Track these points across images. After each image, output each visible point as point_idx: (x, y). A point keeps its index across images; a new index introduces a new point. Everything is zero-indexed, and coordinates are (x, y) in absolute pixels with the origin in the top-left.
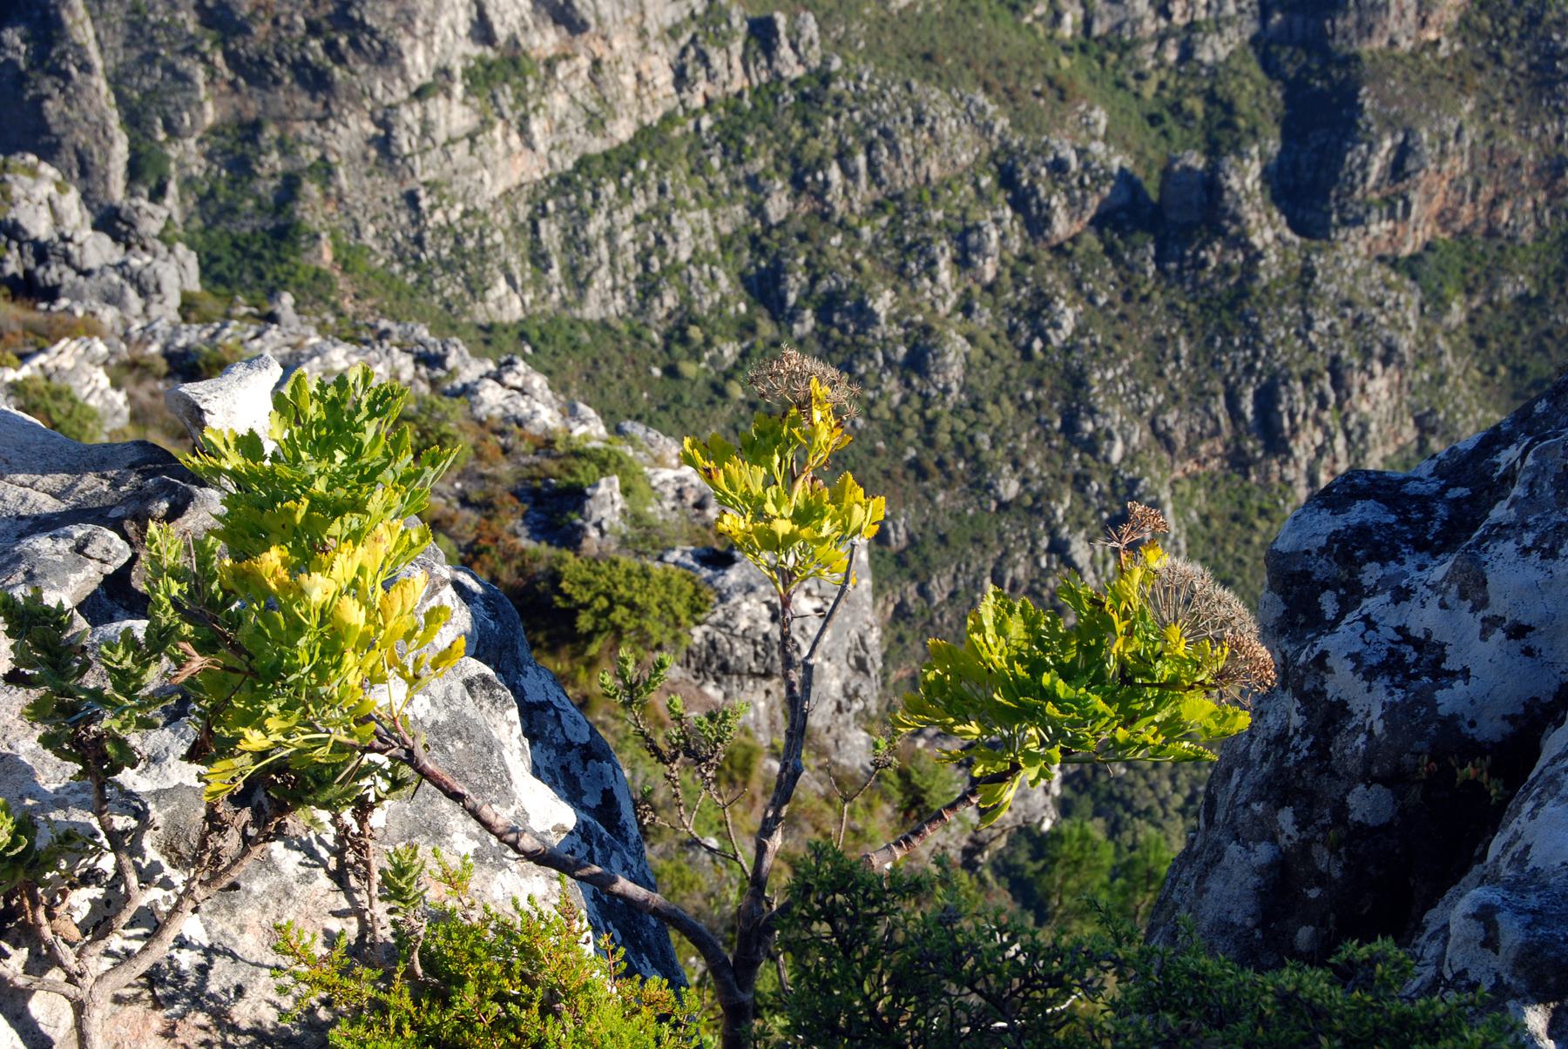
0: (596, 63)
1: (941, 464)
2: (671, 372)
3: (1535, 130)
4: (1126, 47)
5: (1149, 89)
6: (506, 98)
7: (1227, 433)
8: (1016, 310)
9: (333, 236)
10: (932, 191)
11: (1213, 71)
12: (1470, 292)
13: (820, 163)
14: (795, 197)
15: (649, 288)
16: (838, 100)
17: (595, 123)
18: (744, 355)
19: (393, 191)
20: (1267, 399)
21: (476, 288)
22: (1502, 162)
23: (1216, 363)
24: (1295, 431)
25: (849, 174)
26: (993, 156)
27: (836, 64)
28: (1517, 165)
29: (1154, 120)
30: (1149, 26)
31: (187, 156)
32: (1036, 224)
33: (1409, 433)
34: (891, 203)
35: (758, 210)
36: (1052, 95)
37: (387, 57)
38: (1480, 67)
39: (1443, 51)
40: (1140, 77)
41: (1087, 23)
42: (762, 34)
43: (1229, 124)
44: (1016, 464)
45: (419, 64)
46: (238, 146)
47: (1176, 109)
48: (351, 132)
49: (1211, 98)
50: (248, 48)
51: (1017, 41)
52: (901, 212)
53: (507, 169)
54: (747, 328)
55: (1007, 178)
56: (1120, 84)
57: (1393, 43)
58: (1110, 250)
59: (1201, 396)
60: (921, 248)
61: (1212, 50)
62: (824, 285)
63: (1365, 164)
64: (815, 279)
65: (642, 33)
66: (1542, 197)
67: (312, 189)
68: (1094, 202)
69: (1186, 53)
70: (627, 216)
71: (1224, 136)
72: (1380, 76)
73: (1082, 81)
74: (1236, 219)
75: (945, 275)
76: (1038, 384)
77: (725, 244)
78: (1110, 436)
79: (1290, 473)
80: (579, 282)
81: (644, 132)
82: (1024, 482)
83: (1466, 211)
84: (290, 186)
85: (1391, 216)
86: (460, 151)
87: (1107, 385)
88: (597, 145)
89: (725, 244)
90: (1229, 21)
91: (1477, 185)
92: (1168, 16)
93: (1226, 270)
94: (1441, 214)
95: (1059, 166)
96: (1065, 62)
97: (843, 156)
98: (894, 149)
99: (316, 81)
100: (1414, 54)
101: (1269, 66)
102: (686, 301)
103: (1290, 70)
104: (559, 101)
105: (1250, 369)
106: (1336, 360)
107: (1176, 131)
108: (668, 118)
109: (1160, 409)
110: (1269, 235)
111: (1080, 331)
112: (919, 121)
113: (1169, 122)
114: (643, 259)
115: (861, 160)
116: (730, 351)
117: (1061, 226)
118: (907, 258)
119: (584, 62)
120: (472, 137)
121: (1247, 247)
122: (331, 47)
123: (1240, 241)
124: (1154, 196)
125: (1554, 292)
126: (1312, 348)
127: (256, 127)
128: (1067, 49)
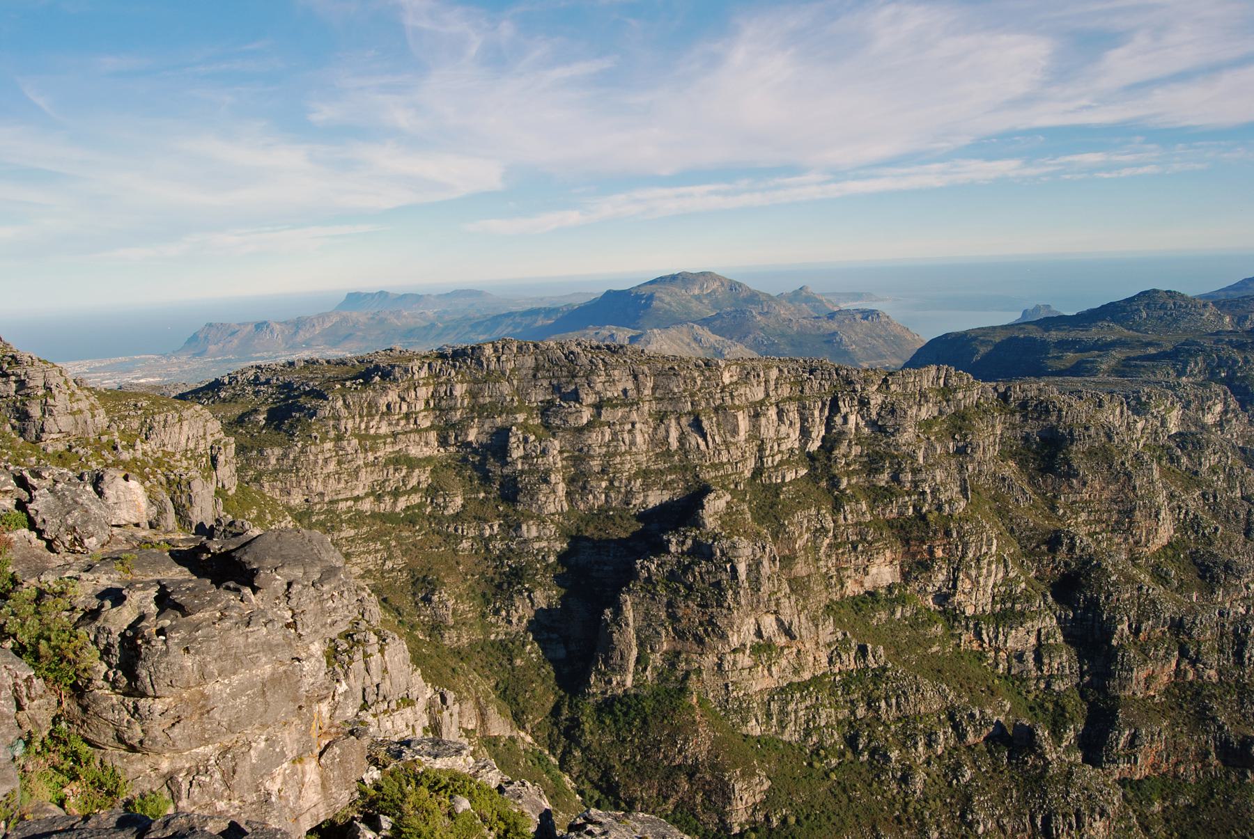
0: (799, 651)
1: (908, 820)
2: (810, 764)
3: (1196, 738)
4: (1024, 680)
5: (1031, 697)
6: (764, 657)
7: (1029, 832)
8: (948, 767)
9: (699, 694)
10: (919, 717)
11: (1059, 694)
12: (1164, 799)
13: (878, 700)
14: (868, 710)
15: (808, 733)
16: (888, 678)
17: (796, 672)
18: (839, 764)
19: (721, 682)
20: (1047, 821)
21: (745, 721)
22: (1180, 748)
23: (1027, 802)
25: (889, 705)
26: (947, 708)
27: (890, 665)
28: (1187, 750)
29: (1032, 709)
30: (1034, 674)
31: (656, 659)
32: (961, 736)
34: (903, 719)
35: (853, 713)
36: (988, 692)
37: (723, 637)
38: (1173, 709)
39: (1157, 700)
40: (1028, 692)
41: (1009, 669)
42: (862, 650)
43: (1063, 715)
44: (938, 826)
45: (735, 640)
46: (673, 658)
47: (1041, 706)
48: (710, 660)
49: (1056, 704)
50: (680, 627)
51: (978, 671)
52: (907, 723)
53: (761, 682)
54: (842, 754)
55: (951, 717)
56: (1019, 693)
57: (1134, 694)
58: (989, 751)
59: (1019, 815)
60: (913, 737)
61: (1058, 686)
62: (873, 744)
63: (1117, 739)
64: (870, 741)
65: (817, 643)
66: (1199, 765)
67: (694, 677)
68: (985, 733)
69: (1048, 685)
70: (803, 706)
71: (1060, 719)
72: (1127, 706)
73: (1003, 690)
74: (1041, 747)
75: (921, 749)
76: (952, 797)
77: (839, 722)
78: (978, 822)
80: (782, 725)
81: (814, 678)
82: (941, 834)
83: (1164, 765)
84: (687, 675)
85: (1129, 762)
86: (746, 672)
87: (980, 802)
88: (796, 679)
89: (839, 722)
90: (1066, 676)
91: (1168, 756)
92: (1042, 671)
93: (1035, 767)
94: (1152, 766)
95: (972, 716)
96: (996, 681)
97: (887, 699)
98: (907, 699)
99: (700, 641)
100: (1143, 699)
101: (1083, 695)
102: (821, 741)
103: (1091, 698)
104: (784, 662)
105: (1041, 807)
106: (1078, 810)
107: (1040, 714)
108: (824, 674)
109: (1001, 816)
110: (1054, 756)
111: (972, 779)
112: (918, 690)
113: (1038, 711)
114: (807, 722)
115: (894, 701)
116: (834, 762)
117: (971, 738)
118: (906, 740)
119: (795, 650)
120: (750, 669)
121: (1045, 759)
122: (706, 630)
123: (1042, 756)
124: (1010, 732)
125: (1203, 806)
126: (1069, 804)
127: (679, 653)
128: (999, 677)
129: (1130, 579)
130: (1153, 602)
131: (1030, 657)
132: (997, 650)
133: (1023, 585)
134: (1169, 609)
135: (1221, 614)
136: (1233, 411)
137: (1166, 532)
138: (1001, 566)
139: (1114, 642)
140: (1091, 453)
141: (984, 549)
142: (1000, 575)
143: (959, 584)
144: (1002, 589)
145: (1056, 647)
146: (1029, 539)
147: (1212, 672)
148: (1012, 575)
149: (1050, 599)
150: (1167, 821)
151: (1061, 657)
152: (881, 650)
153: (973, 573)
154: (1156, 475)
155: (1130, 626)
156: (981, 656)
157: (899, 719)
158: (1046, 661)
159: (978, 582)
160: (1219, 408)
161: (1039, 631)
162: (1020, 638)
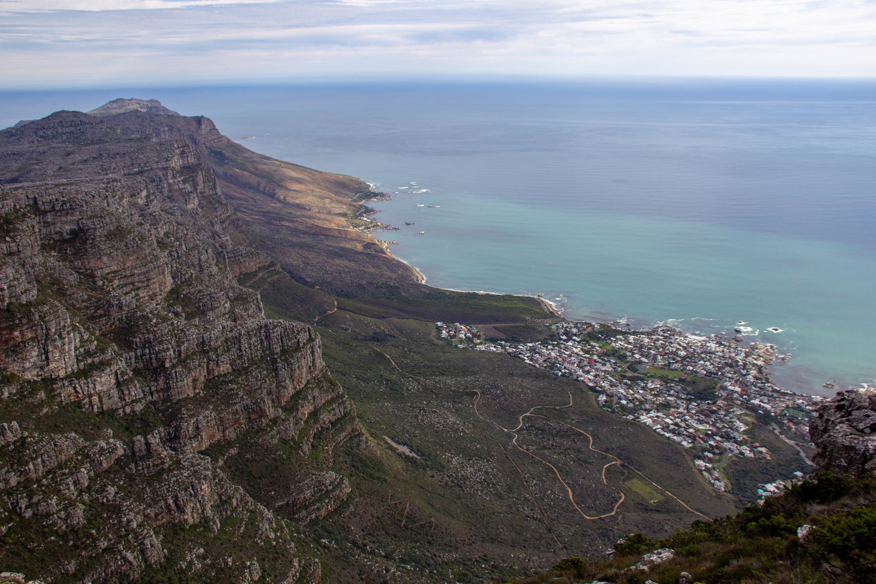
24: (185, 506)
33: (216, 497)
39: (201, 394)
75: (72, 488)
79: (186, 517)
95: (102, 448)
109: (145, 509)
115: (40, 460)
129: (165, 319)
130: (182, 330)
131: (115, 392)
132: (90, 396)
133: (96, 343)
134: (193, 334)
135: (223, 327)
136: (153, 194)
137: (169, 282)
138: (77, 335)
139: (168, 365)
140: (110, 236)
141: (62, 323)
142: (78, 340)
143: (50, 355)
144: (82, 350)
145: (131, 380)
146: (87, 308)
147: (228, 366)
148: (86, 337)
149: (116, 348)
150: (230, 467)
151: (135, 386)
152: (15, 424)
153: (59, 343)
154: (156, 244)
155: (174, 351)
156: (78, 405)
157: (48, 472)
158: (126, 392)
159: (64, 350)
160: (144, 193)
161: (116, 372)
162: (104, 381)
